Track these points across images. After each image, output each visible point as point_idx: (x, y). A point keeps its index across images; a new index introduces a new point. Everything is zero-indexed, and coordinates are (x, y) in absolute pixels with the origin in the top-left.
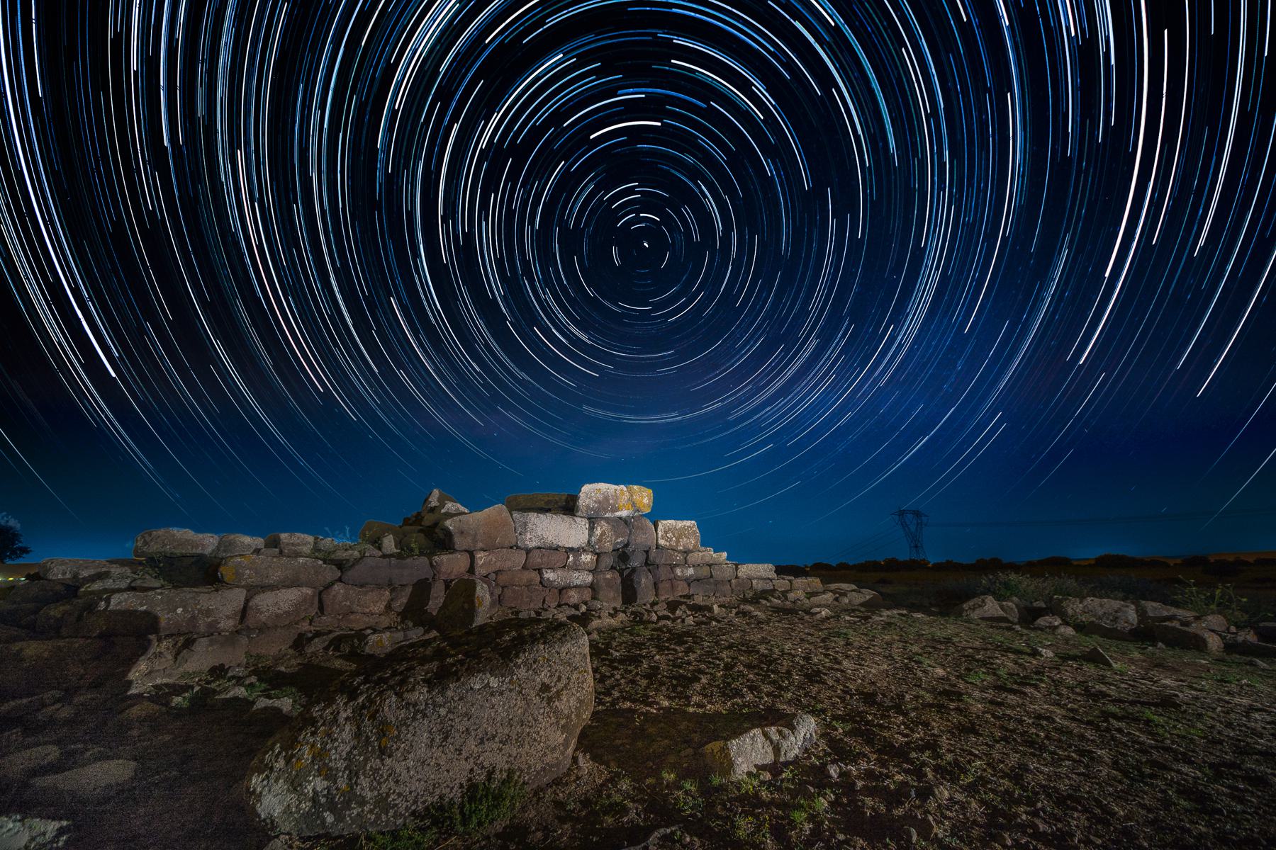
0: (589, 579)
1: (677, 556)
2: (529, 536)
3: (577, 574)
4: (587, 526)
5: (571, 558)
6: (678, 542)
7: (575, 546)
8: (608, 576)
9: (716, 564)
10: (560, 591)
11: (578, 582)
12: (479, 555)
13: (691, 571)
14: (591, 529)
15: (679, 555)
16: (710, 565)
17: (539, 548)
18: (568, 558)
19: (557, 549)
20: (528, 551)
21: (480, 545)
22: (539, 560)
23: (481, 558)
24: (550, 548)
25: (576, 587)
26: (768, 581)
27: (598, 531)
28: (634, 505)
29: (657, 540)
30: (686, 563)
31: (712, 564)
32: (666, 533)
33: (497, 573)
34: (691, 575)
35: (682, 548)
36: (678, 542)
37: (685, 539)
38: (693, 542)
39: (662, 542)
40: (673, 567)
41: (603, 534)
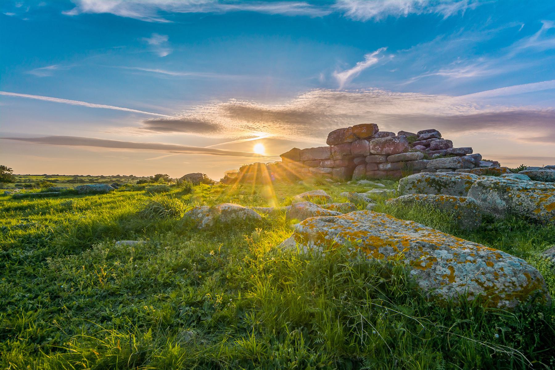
1: (380, 158)
6: (381, 151)
8: (338, 170)
13: (389, 166)
15: (382, 158)
30: (387, 162)
32: (375, 146)
34: (389, 169)
35: (384, 153)
38: (392, 149)
39: (372, 151)
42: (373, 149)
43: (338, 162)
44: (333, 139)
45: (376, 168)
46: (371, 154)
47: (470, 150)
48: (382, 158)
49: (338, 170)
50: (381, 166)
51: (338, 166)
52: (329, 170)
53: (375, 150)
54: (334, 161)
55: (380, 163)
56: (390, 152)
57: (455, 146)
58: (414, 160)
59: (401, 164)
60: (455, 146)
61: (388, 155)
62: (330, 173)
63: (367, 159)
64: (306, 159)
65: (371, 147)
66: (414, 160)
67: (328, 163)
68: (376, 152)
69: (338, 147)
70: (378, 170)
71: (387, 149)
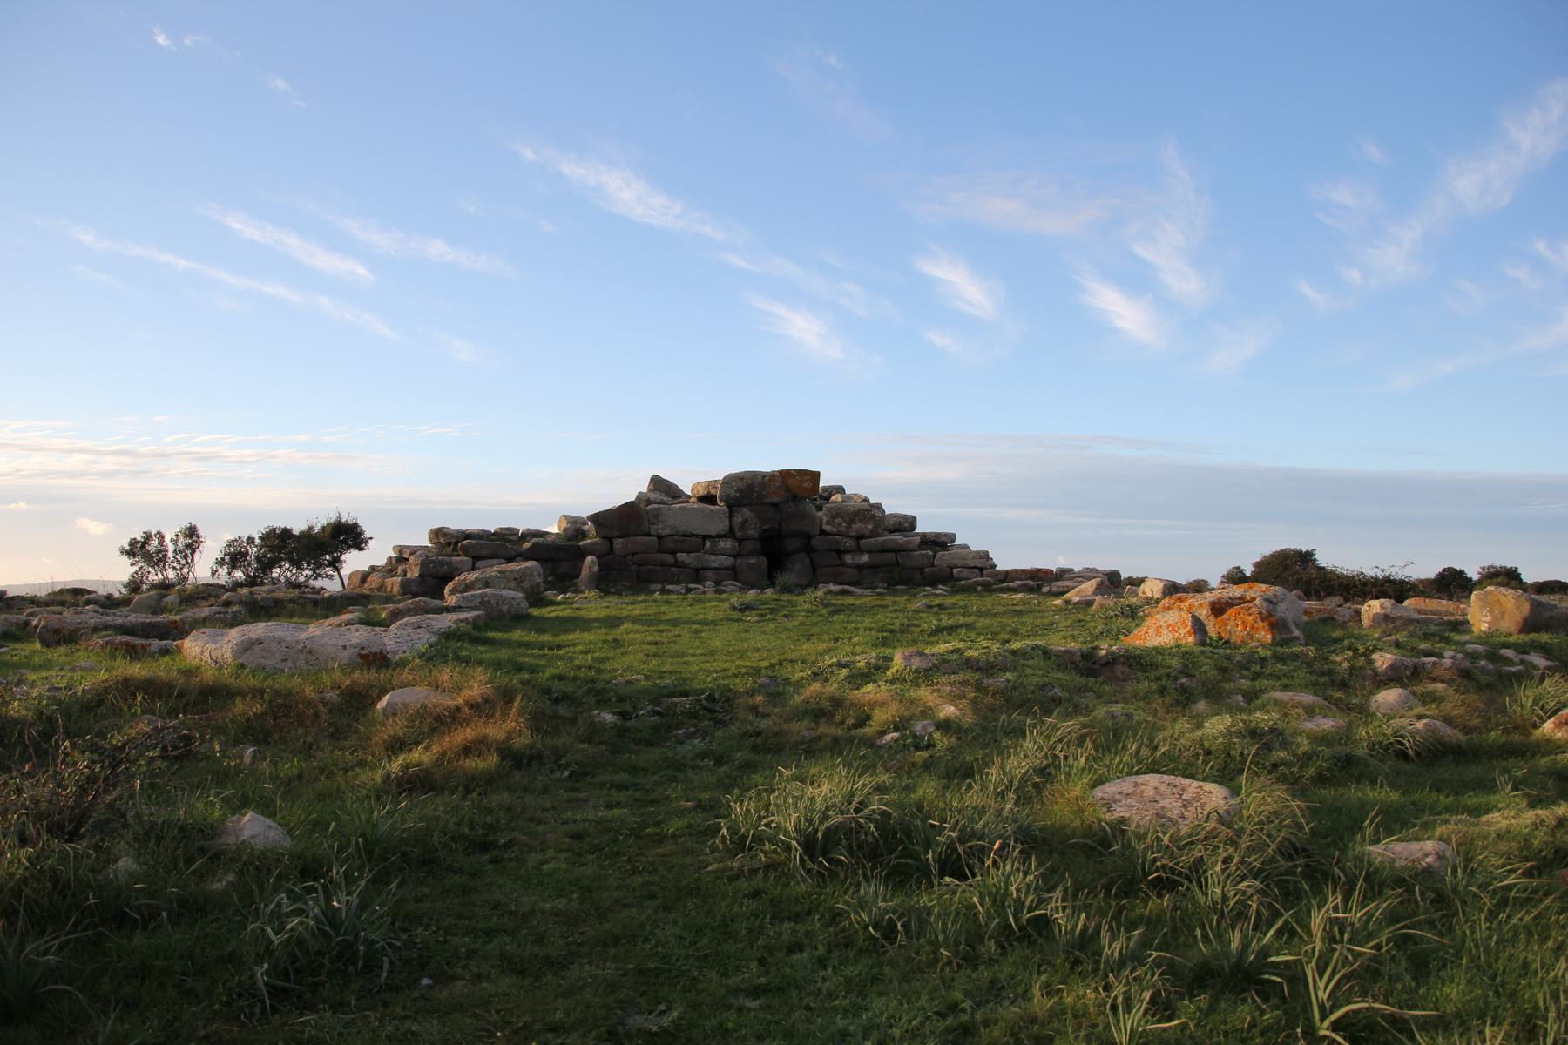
0: (729, 561)
2: (661, 526)
3: (713, 557)
4: (727, 515)
5: (708, 544)
6: (848, 528)
7: (713, 532)
9: (904, 551)
10: (697, 570)
11: (716, 565)
12: (616, 541)
13: (865, 558)
14: (731, 517)
16: (896, 551)
17: (672, 535)
18: (704, 544)
19: (692, 535)
20: (660, 537)
21: (616, 533)
22: (672, 546)
23: (619, 543)
24: (684, 536)
25: (715, 569)
26: (975, 570)
27: (738, 519)
28: (788, 489)
29: (821, 526)
31: (899, 551)
32: (833, 518)
33: (633, 554)
35: (854, 534)
36: (848, 528)
37: (859, 525)
39: (827, 528)
40: (840, 553)
41: (745, 521)
42: (828, 523)
43: (749, 546)
44: (737, 491)
45: (838, 562)
46: (823, 532)
47: (952, 537)
48: (850, 543)
49: (752, 561)
50: (848, 559)
51: (750, 554)
52: (729, 561)
53: (834, 526)
54: (740, 541)
55: (846, 552)
56: (867, 533)
57: (921, 528)
58: (911, 551)
59: (890, 557)
60: (921, 528)
61: (860, 537)
62: (733, 569)
63: (817, 542)
64: (667, 532)
65: (825, 519)
66: (911, 551)
67: (726, 544)
68: (835, 530)
69: (751, 510)
70: (843, 564)
71: (857, 527)
